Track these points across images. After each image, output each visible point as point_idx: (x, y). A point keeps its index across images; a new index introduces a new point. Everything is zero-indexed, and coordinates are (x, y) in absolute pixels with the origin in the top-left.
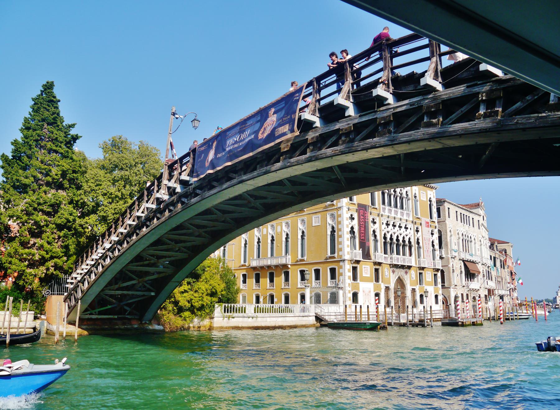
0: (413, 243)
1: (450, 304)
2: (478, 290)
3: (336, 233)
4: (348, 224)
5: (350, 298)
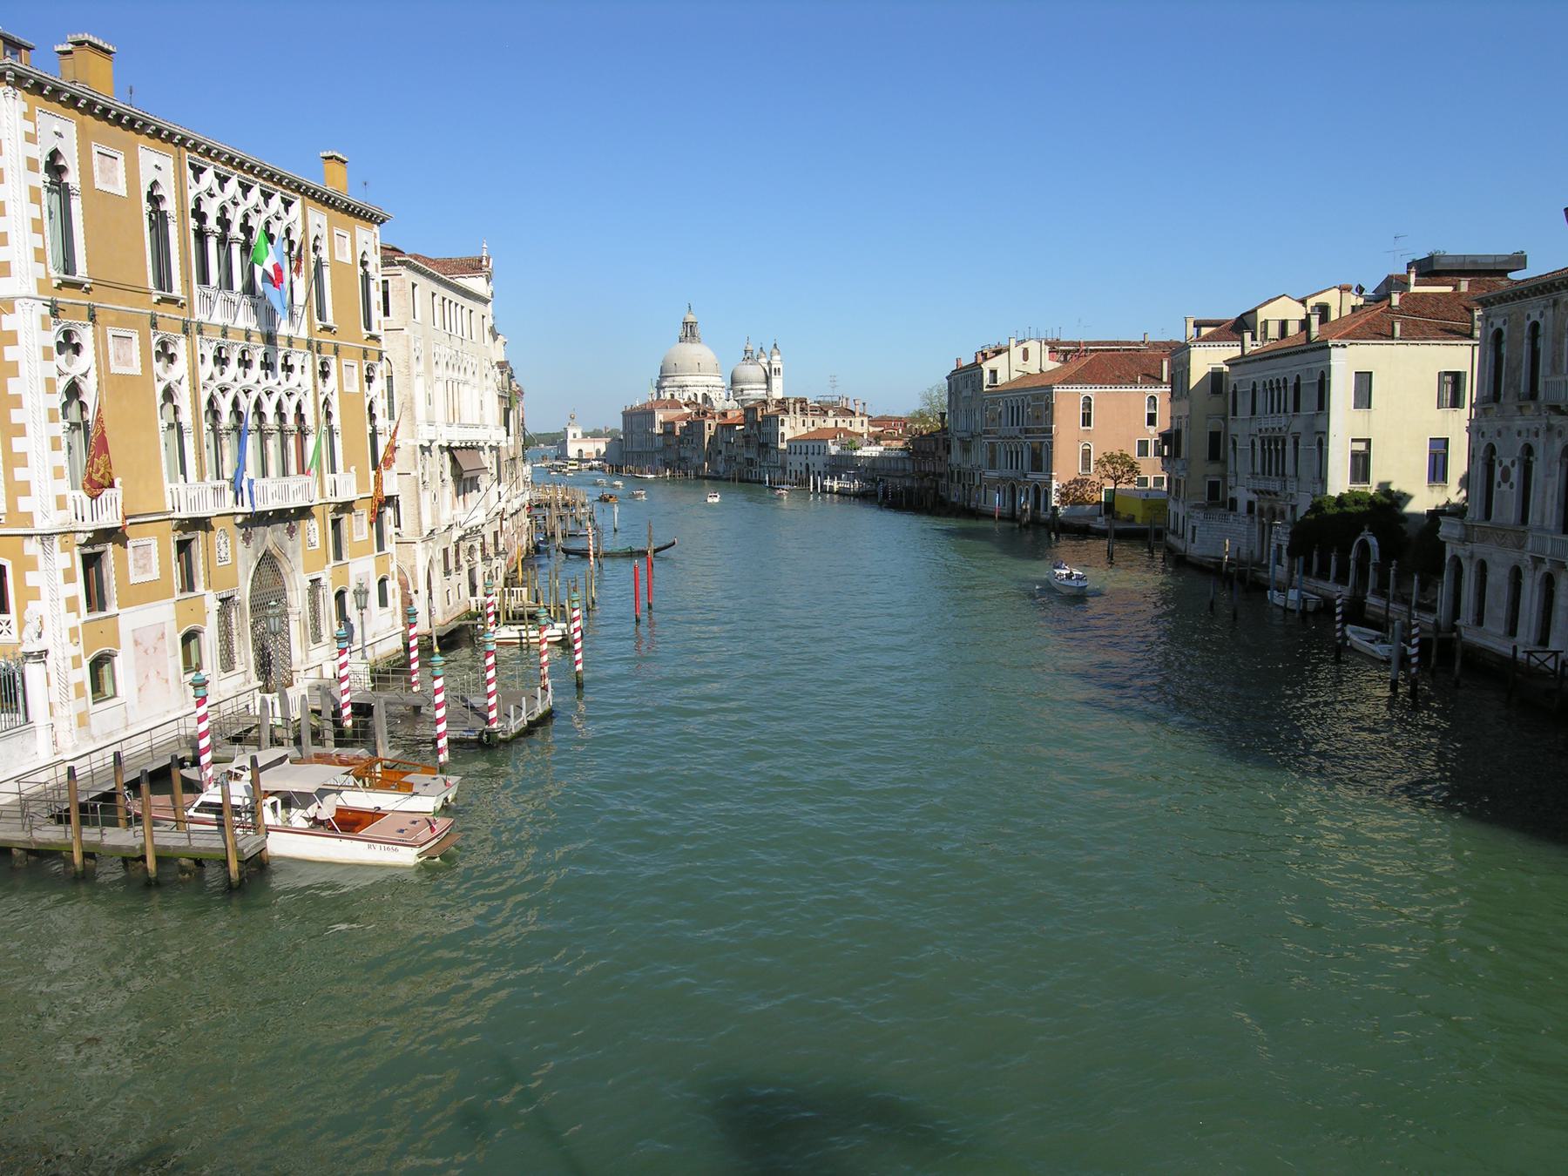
0: (310, 421)
1: (416, 592)
5: (79, 687)
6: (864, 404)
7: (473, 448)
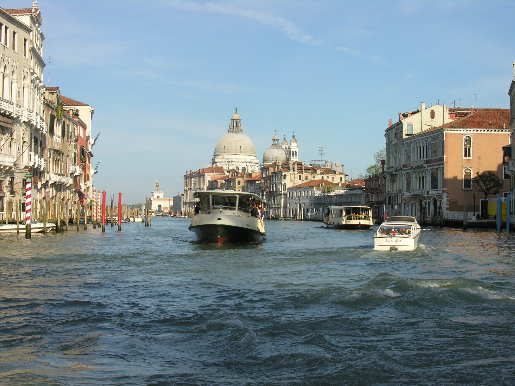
6: (342, 166)
7: (9, 117)
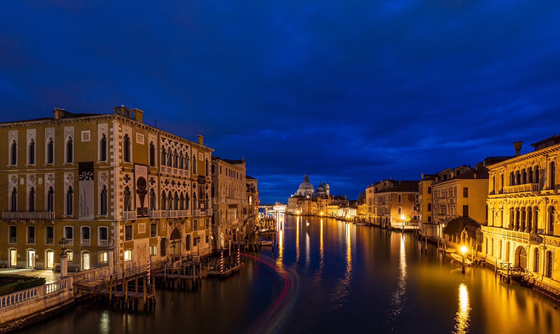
0: (190, 197)
2: (238, 224)
3: (107, 194)
4: (122, 184)
